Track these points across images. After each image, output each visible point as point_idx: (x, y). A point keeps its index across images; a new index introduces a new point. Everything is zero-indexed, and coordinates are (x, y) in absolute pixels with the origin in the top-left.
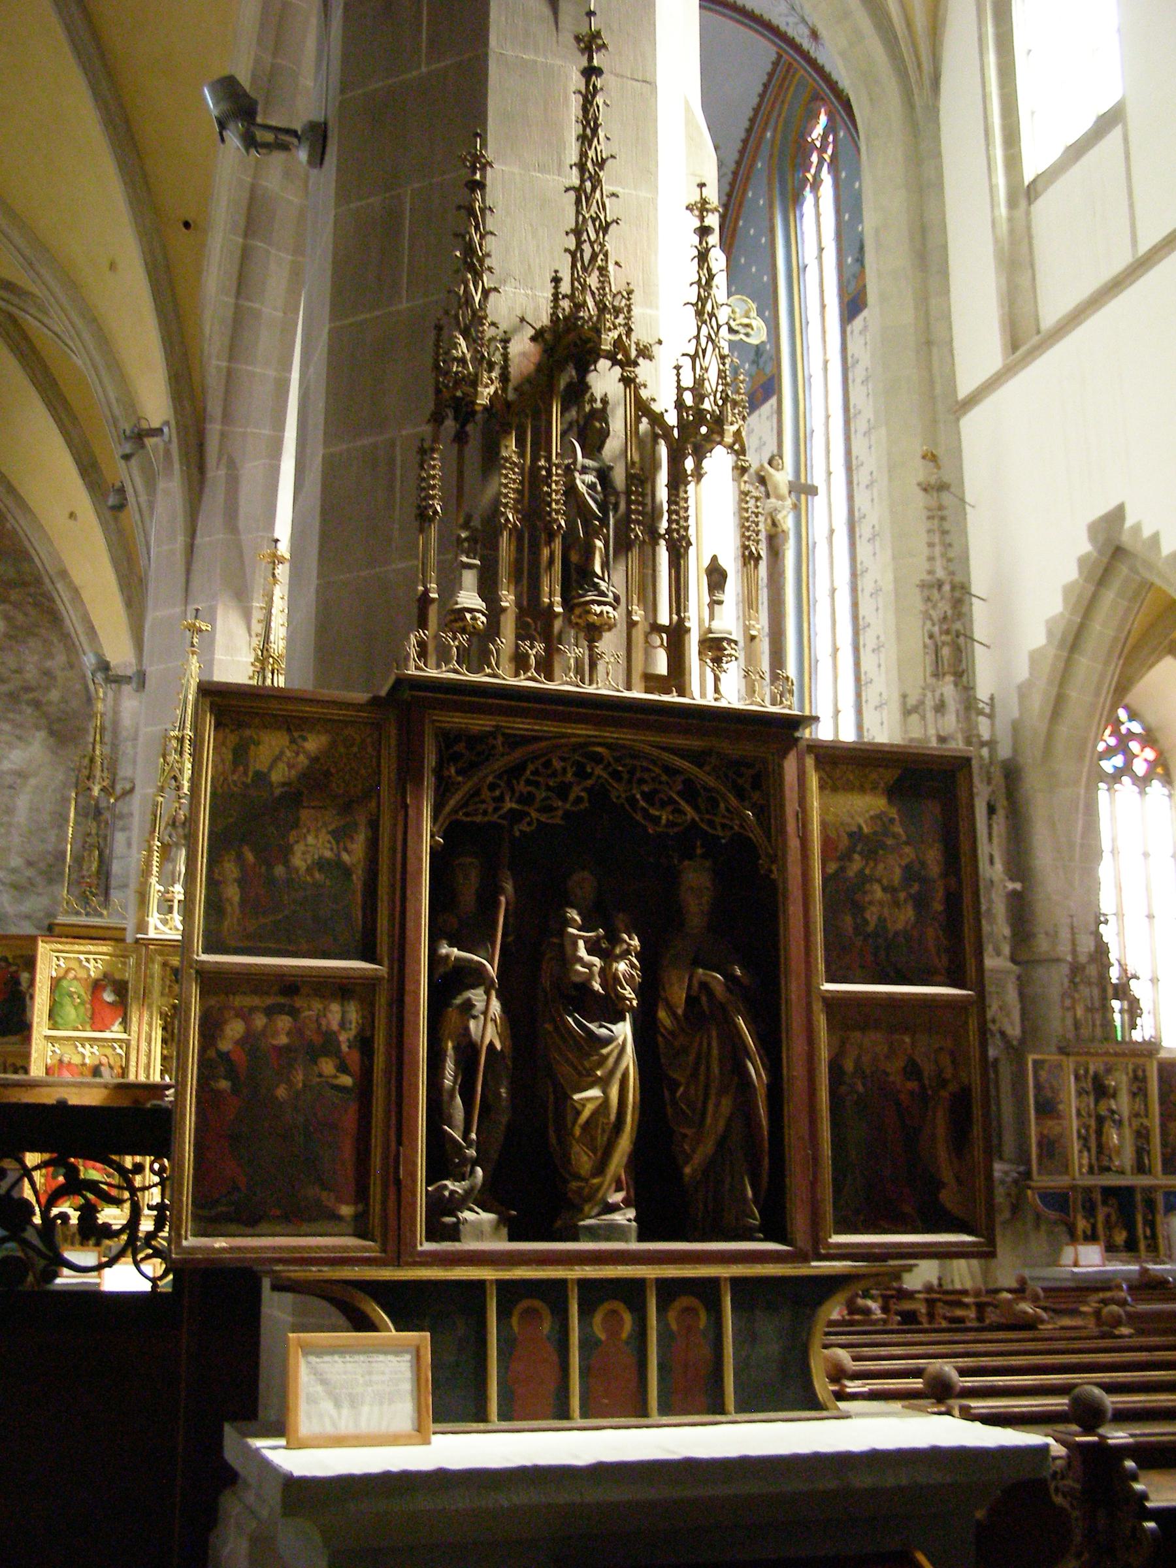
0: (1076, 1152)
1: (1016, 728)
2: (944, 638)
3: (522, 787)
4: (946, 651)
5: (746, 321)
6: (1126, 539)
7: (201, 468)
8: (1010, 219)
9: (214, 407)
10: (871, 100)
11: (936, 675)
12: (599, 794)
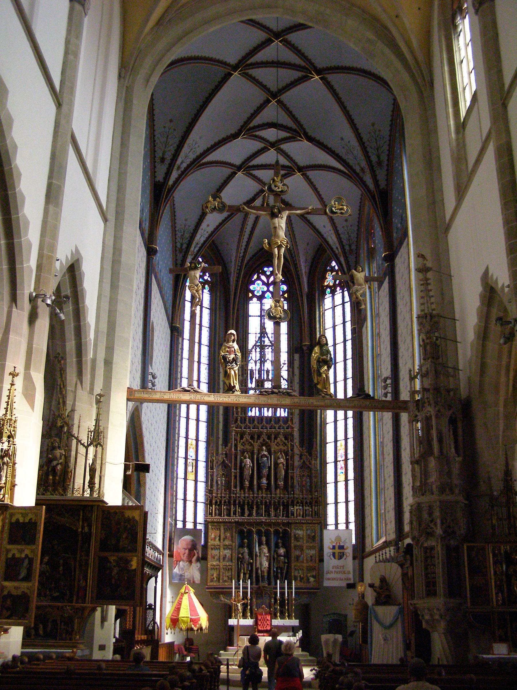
0: (494, 593)
1: (469, 379)
2: (428, 341)
4: (428, 347)
5: (341, 207)
6: (490, 282)
8: (457, 139)
10: (405, 99)
11: (424, 359)
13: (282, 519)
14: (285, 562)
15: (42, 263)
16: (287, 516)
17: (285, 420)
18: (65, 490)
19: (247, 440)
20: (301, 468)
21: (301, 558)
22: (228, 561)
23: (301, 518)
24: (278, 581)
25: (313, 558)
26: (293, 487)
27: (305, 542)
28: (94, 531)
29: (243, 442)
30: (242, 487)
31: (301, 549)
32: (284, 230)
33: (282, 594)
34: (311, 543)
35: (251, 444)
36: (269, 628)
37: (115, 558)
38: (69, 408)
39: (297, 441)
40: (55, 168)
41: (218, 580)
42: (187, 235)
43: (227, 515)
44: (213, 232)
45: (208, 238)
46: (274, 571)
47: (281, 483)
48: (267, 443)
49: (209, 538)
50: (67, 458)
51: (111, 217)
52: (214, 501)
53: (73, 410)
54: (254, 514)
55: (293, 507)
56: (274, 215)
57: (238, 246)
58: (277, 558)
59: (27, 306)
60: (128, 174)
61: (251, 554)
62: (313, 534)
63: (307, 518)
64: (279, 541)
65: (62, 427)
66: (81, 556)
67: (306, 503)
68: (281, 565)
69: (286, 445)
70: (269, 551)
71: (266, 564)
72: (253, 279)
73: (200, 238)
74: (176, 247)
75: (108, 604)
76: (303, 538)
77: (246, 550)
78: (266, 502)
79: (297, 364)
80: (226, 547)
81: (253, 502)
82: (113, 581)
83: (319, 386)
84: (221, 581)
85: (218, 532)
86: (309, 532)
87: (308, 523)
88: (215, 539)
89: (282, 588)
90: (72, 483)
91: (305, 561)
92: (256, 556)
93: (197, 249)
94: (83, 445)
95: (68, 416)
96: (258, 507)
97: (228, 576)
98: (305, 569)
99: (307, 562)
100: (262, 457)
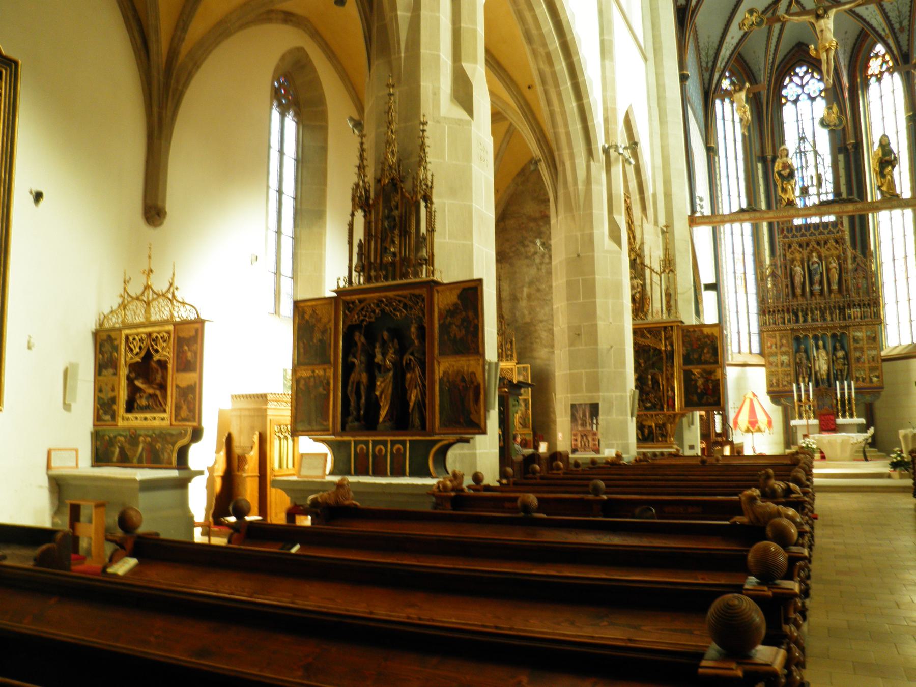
3: (364, 313)
7: (555, 168)
9: (554, 147)
12: (383, 311)
13: (837, 322)
14: (844, 364)
15: (608, 117)
16: (844, 319)
17: (834, 224)
18: (646, 315)
19: (795, 249)
20: (856, 270)
21: (862, 360)
22: (786, 367)
23: (859, 320)
24: (837, 382)
25: (875, 358)
26: (848, 290)
27: (865, 343)
28: (675, 347)
29: (792, 252)
30: (794, 295)
31: (861, 350)
32: (832, 31)
33: (843, 395)
34: (872, 344)
35: (800, 252)
36: (833, 427)
37: (699, 371)
38: (638, 241)
39: (848, 243)
40: (604, 24)
41: (778, 385)
42: (712, 53)
43: (781, 323)
44: (738, 44)
45: (733, 51)
46: (834, 373)
47: (835, 287)
48: (817, 249)
49: (766, 346)
50: (644, 286)
51: (650, 55)
52: (767, 311)
53: (642, 243)
54: (809, 319)
55: (850, 310)
56: (819, 17)
57: (766, 52)
58: (836, 361)
59: (602, 157)
60: (660, 10)
61: (808, 359)
62: (874, 335)
63: (866, 319)
64: (837, 344)
65: (635, 260)
66: (667, 370)
67: (864, 305)
68: (840, 367)
69: (837, 249)
70: (827, 354)
71: (825, 368)
72: (785, 84)
73: (725, 52)
74: (701, 66)
75: (692, 411)
76: (862, 340)
77: (803, 355)
78: (821, 307)
79: (841, 165)
80: (783, 353)
81: (807, 309)
82: (699, 391)
83: (882, 189)
84: (781, 386)
85: (774, 340)
86: (869, 333)
87: (867, 325)
88: (771, 347)
89: (842, 389)
90: (650, 308)
91: (867, 362)
92: (814, 360)
93: (723, 64)
94: (657, 273)
95: (639, 249)
96: (812, 313)
97: (787, 382)
98: (867, 370)
99: (869, 362)
100: (812, 264)
